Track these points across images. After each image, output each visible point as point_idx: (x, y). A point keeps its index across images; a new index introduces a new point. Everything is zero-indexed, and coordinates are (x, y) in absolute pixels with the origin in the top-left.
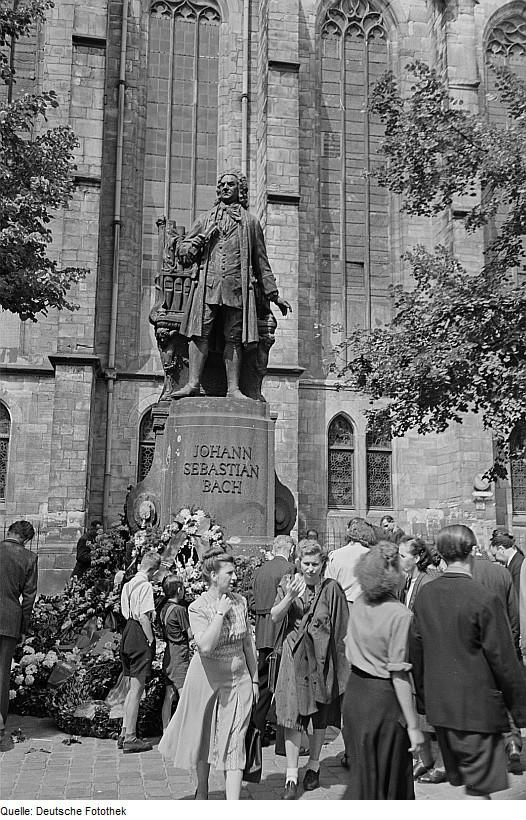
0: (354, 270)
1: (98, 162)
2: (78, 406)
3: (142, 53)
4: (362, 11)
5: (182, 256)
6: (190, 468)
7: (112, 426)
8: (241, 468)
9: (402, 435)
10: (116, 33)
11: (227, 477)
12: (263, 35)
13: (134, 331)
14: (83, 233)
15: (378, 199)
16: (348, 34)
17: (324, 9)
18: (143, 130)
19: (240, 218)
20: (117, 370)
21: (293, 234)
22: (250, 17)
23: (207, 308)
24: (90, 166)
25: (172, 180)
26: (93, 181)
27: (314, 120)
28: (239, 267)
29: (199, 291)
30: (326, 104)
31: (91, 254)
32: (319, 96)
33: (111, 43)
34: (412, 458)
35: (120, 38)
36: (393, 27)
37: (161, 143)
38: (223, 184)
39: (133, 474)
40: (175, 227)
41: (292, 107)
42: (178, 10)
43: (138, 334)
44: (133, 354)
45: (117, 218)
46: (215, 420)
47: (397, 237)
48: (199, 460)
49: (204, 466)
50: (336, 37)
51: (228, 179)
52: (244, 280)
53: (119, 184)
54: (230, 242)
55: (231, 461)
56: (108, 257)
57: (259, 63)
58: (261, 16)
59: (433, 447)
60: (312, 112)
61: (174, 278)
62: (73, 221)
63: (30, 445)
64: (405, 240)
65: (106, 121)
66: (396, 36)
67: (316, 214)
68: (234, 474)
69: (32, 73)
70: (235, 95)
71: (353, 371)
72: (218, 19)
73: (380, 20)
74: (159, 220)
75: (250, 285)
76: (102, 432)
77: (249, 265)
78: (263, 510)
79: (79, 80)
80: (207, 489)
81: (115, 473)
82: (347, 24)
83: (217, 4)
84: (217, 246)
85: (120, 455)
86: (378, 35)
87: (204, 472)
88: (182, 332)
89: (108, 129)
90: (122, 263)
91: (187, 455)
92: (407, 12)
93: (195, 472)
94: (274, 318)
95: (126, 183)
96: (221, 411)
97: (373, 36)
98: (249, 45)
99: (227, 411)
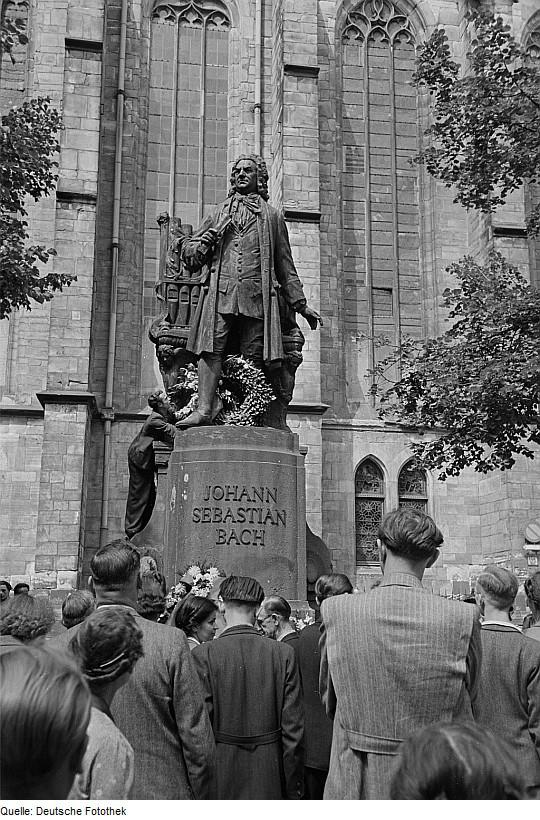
0: (381, 297)
1: (94, 177)
2: (70, 451)
5: (189, 258)
6: (201, 515)
7: (108, 472)
8: (264, 514)
9: (457, 474)
10: (114, 39)
11: (246, 526)
12: (277, 39)
13: (134, 367)
14: (76, 256)
16: (371, 39)
17: (344, 12)
18: (143, 149)
19: (259, 210)
20: (115, 410)
21: (313, 255)
22: (262, 21)
23: (220, 319)
25: (177, 199)
26: (88, 198)
27: (336, 132)
28: (259, 269)
29: (211, 297)
30: (348, 115)
31: (86, 279)
32: (340, 107)
33: (108, 50)
34: (452, 506)
35: (119, 44)
36: (421, 31)
38: (239, 171)
40: (180, 226)
41: (311, 115)
42: (182, 14)
43: (138, 371)
44: (133, 392)
45: (116, 241)
46: (231, 454)
47: (429, 260)
48: (211, 504)
49: (218, 512)
51: (244, 164)
52: (265, 284)
54: (248, 239)
55: (252, 505)
56: (105, 283)
57: (272, 70)
58: (274, 19)
59: (475, 495)
60: (333, 124)
61: (180, 286)
62: (65, 242)
63: (16, 496)
65: (103, 134)
67: (338, 235)
68: (256, 519)
69: (21, 84)
71: (399, 394)
72: (226, 24)
73: (407, 24)
74: (161, 217)
75: (273, 290)
76: (98, 481)
77: (270, 266)
78: (292, 566)
79: (72, 87)
80: (222, 540)
82: (369, 28)
83: (225, 7)
84: (231, 244)
86: (404, 40)
87: (218, 519)
88: (189, 348)
91: (195, 498)
93: (207, 519)
94: (300, 332)
95: (125, 202)
97: (399, 42)
98: (262, 52)
99: (245, 442)
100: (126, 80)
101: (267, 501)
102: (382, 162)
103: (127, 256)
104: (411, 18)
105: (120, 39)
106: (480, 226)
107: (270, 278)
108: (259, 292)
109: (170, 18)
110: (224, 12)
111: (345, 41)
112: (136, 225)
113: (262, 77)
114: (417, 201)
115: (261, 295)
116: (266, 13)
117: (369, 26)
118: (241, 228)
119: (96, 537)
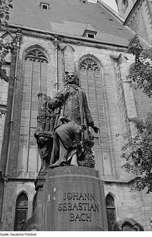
1: (6, 100)
3: (22, 70)
4: (92, 63)
5: (51, 105)
6: (62, 207)
7: (5, 200)
11: (83, 212)
13: (16, 162)
15: (101, 117)
16: (88, 69)
18: (21, 95)
20: (8, 177)
22: (58, 62)
24: (3, 101)
25: (32, 109)
28: (79, 108)
30: (82, 88)
31: (1, 131)
34: (123, 210)
35: (15, 66)
36: (101, 68)
37: (28, 98)
39: (13, 222)
40: (46, 97)
42: (34, 59)
43: (17, 163)
44: (15, 171)
46: (74, 178)
49: (70, 205)
50: (84, 69)
52: (81, 114)
53: (13, 110)
54: (74, 98)
55: (85, 202)
56: (7, 134)
59: (131, 206)
61: (46, 117)
64: (112, 130)
66: (102, 70)
68: (87, 209)
70: (53, 84)
71: (133, 158)
73: (97, 66)
74: (39, 94)
75: (84, 116)
80: (72, 219)
81: (5, 222)
83: (47, 58)
84: (68, 99)
85: (8, 213)
86: (97, 70)
87: (70, 208)
89: (10, 92)
90: (12, 136)
91: (59, 199)
95: (15, 109)
96: (77, 174)
97: (95, 70)
98: (58, 70)
99: (80, 173)
101: (91, 200)
102: (93, 101)
103: (15, 125)
104: (98, 64)
105: (16, 64)
106: (124, 119)
107: (83, 113)
108: (79, 116)
109: (30, 60)
110: (46, 59)
111: (80, 69)
112: (18, 116)
113: (58, 76)
114: (104, 112)
115: (80, 118)
116: (59, 60)
117: (87, 65)
118: (72, 94)
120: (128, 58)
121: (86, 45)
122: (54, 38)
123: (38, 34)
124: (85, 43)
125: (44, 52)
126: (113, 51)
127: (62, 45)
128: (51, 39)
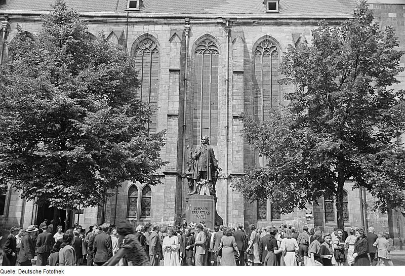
2: (172, 188)
10: (184, 62)
14: (173, 132)
26: (176, 116)
36: (280, 50)
45: (184, 124)
53: (185, 113)
57: (231, 72)
62: (170, 128)
63: (158, 199)
65: (180, 92)
76: (180, 195)
78: (212, 223)
82: (264, 50)
83: (217, 47)
92: (285, 45)
95: (187, 112)
98: (228, 62)
100: (187, 75)
103: (188, 128)
116: (230, 50)
119: (180, 211)
120: (308, 42)
121: (263, 24)
122: (225, 22)
123: (207, 21)
124: (262, 21)
125: (215, 41)
126: (296, 26)
127: (235, 29)
128: (222, 24)
